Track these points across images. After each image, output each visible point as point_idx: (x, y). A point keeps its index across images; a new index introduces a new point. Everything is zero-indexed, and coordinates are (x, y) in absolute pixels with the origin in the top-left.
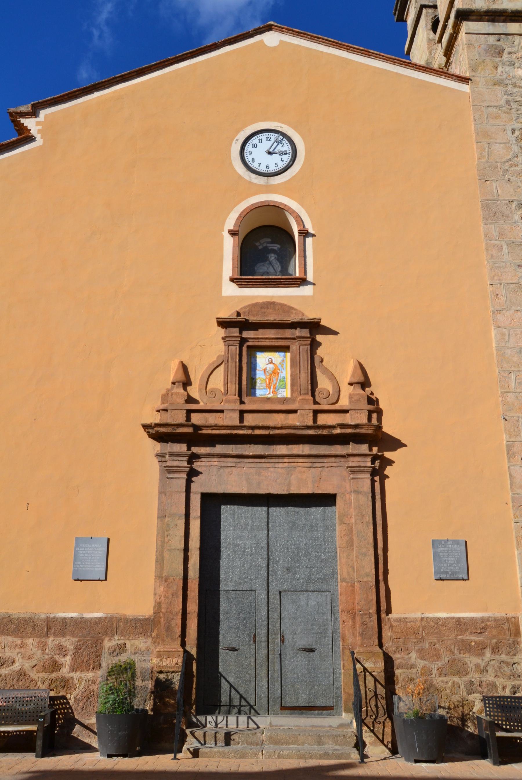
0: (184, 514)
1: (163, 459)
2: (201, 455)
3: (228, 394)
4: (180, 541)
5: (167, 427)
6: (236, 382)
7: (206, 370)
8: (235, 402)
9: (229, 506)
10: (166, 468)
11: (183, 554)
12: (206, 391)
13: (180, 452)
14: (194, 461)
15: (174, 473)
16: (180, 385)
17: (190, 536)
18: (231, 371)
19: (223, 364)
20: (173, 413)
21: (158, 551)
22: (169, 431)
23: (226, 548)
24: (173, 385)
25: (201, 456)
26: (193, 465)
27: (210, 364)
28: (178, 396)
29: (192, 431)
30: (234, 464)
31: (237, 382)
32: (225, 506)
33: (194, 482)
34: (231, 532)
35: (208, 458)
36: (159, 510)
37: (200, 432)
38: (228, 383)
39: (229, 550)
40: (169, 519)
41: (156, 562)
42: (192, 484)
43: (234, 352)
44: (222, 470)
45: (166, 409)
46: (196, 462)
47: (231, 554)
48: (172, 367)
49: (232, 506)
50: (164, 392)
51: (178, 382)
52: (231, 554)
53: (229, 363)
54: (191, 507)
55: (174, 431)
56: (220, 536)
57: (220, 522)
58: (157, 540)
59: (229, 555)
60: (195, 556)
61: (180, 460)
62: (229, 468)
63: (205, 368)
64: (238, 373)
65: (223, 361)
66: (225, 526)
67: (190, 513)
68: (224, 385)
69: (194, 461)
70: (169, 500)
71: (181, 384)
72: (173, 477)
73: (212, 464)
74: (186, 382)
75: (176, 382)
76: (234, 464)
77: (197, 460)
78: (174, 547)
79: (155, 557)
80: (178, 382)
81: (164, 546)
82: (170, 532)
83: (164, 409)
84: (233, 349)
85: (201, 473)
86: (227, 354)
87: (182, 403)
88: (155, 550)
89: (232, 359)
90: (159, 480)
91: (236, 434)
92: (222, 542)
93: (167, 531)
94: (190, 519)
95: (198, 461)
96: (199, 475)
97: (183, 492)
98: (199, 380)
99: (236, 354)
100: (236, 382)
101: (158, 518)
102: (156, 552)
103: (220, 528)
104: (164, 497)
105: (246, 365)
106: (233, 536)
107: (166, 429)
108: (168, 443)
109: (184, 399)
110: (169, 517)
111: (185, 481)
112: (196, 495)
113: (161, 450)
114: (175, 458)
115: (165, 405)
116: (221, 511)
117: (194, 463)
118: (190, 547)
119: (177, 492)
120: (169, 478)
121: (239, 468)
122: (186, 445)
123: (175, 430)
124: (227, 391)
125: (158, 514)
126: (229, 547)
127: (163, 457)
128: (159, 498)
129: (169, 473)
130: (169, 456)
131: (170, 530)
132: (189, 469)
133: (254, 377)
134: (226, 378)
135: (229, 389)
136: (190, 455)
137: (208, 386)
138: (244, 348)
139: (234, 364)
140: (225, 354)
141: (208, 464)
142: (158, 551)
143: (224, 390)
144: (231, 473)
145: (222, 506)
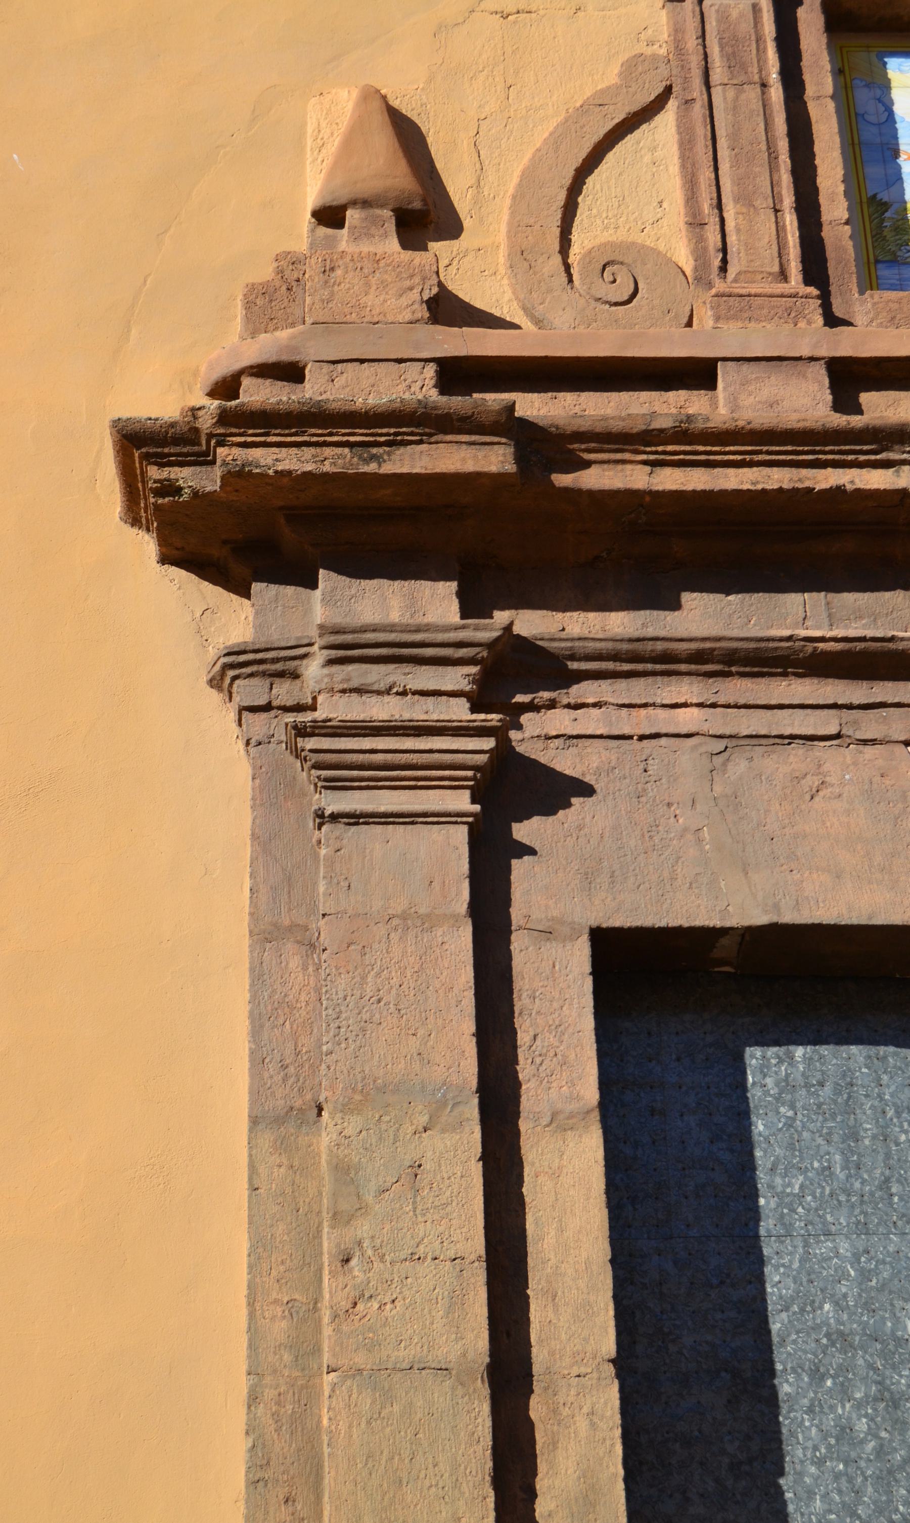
0: (474, 1083)
1: (284, 692)
2: (573, 657)
3: (732, 271)
4: (456, 1301)
5: (313, 433)
6: (776, 197)
7: (556, 140)
8: (793, 316)
9: (799, 1052)
10: (311, 743)
11: (486, 1408)
12: (567, 268)
13: (418, 630)
14: (520, 698)
15: (373, 785)
16: (379, 223)
17: (531, 1261)
18: (734, 136)
19: (672, 105)
20: (340, 381)
21: (269, 1394)
22: (327, 468)
23: (817, 1376)
24: (323, 231)
25: (574, 665)
26: (514, 735)
27: (583, 109)
28: (373, 281)
29: (510, 467)
30: (828, 723)
31: (788, 200)
32: (772, 1051)
33: (532, 852)
34: (844, 1247)
35: (622, 684)
36: (258, 1062)
37: (562, 480)
38: (719, 206)
39: (844, 1392)
40: (353, 1124)
41: (253, 1483)
42: (519, 867)
43: (746, 27)
44: (739, 766)
45: (286, 357)
46: (532, 707)
47: (862, 1425)
48: (310, 129)
49: (825, 1050)
50: (265, 273)
51: (365, 203)
52: (862, 1425)
53: (717, 93)
54: (523, 1038)
55: (372, 467)
56: (760, 1280)
57: (748, 1166)
58: (251, 1304)
59: (845, 1431)
60: (582, 1424)
61: (413, 685)
62: (797, 751)
63: (541, 134)
64: (783, 145)
65: (668, 90)
66: (788, 1202)
67: (519, 1085)
68: (696, 224)
69: (520, 698)
70: (342, 982)
71: (387, 214)
72: (369, 808)
73: (662, 720)
74: (417, 205)
75: (354, 203)
76: (828, 723)
77: (546, 695)
78: (404, 1355)
79: (240, 1446)
80: (365, 203)
81: (317, 1350)
82: (363, 1228)
83: (273, 359)
84: (734, 14)
85: (586, 790)
86: (692, 42)
87: (408, 316)
88: (242, 1385)
89: (734, 62)
90: (254, 837)
91: (839, 490)
92: (775, 1327)
93: (338, 1218)
94: (524, 1125)
95: (552, 705)
96: (569, 805)
97: (455, 917)
98: (508, 202)
99: (759, 39)
100: (776, 197)
101: (254, 1121)
102: (253, 1399)
103: (754, 1214)
104: (294, 962)
105: (831, 106)
106: (865, 1275)
107: (309, 452)
108: (312, 583)
109: (415, 295)
110: (347, 1109)
111: (460, 835)
112: (552, 950)
113: (259, 627)
114: (376, 675)
115: (284, 335)
116: (742, 1086)
117: (525, 718)
118: (539, 1356)
119: (404, 917)
120: (335, 817)
121: (869, 751)
122: (453, 586)
123: (373, 458)
124: (724, 250)
125: (257, 1093)
126: (843, 1369)
127: (281, 675)
128: (258, 976)
129: (333, 785)
130: (331, 662)
131: (362, 1209)
132: (489, 743)
133: (884, 196)
134: (706, 175)
135: (732, 239)
136: (491, 645)
137: (575, 237)
138: (801, 12)
139: (752, 94)
140: (679, 48)
141: (627, 723)
142: (269, 1394)
143: (700, 254)
144: (812, 781)
145: (748, 1051)
